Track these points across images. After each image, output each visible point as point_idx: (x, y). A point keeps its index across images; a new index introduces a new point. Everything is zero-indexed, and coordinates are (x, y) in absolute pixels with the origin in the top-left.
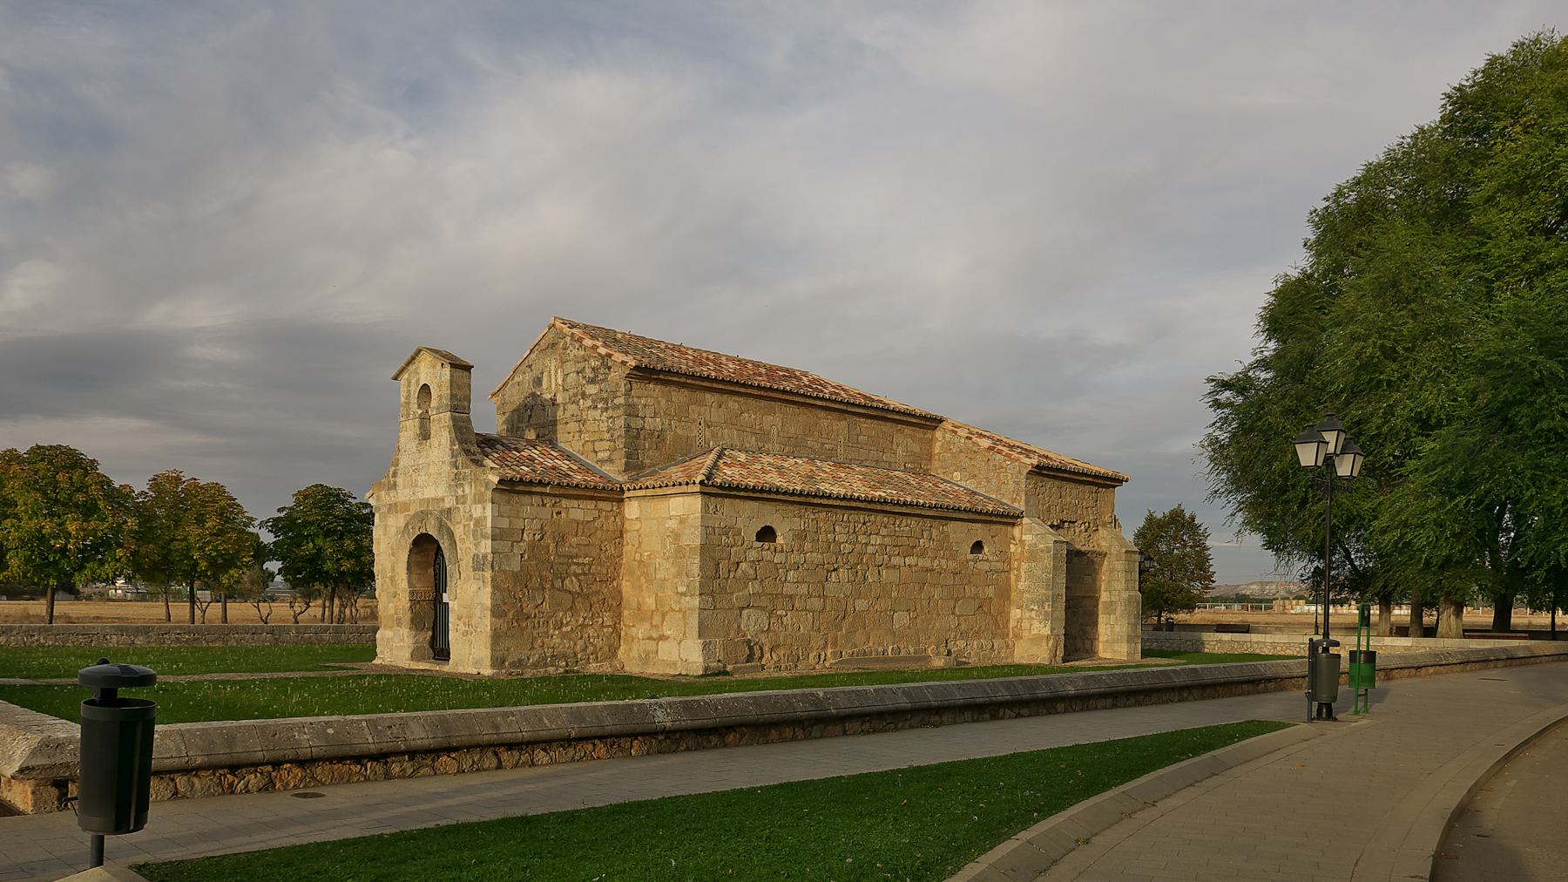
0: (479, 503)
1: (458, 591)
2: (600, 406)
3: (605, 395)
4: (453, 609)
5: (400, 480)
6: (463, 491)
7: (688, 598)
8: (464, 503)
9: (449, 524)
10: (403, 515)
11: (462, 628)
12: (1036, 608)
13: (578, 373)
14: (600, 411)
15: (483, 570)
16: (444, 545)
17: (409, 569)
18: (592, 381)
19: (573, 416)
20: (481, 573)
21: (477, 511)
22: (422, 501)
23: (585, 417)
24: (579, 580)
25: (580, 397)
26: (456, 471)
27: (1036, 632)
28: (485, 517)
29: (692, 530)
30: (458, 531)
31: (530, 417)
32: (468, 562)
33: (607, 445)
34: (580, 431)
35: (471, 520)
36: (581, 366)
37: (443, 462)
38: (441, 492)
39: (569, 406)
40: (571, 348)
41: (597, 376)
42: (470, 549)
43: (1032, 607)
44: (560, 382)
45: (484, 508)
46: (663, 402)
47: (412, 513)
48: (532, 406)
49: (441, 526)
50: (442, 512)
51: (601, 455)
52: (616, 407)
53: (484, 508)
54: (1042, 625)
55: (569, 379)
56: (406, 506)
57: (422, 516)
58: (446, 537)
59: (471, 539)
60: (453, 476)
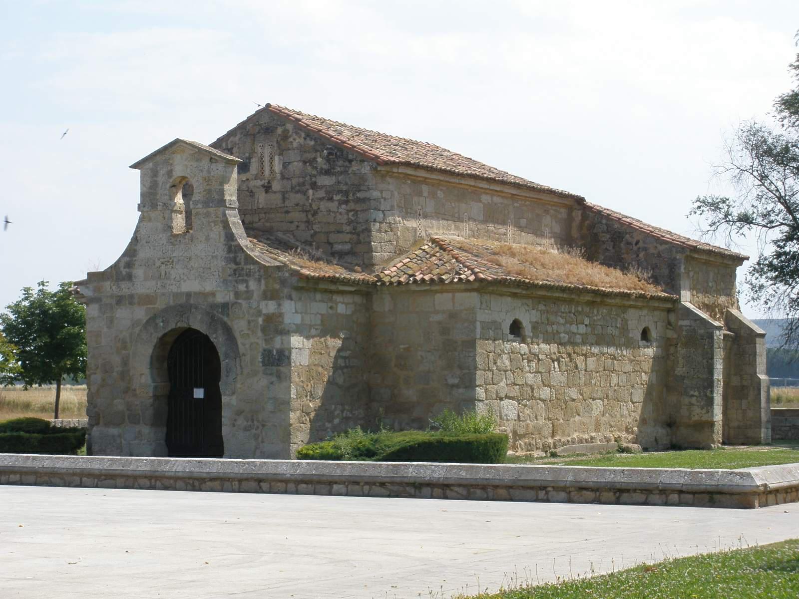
0: (272, 299)
2: (335, 198)
3: (344, 188)
6: (247, 287)
7: (461, 390)
9: (225, 319)
10: (145, 307)
11: (241, 422)
12: (696, 394)
13: (305, 162)
14: (336, 203)
15: (278, 365)
16: (218, 340)
17: (151, 363)
18: (327, 172)
19: (297, 205)
20: (274, 368)
21: (270, 307)
22: (176, 295)
23: (314, 207)
24: (343, 373)
25: (308, 187)
26: (234, 267)
27: (696, 418)
29: (466, 324)
30: (239, 326)
33: (347, 237)
34: (308, 222)
35: (260, 316)
36: (309, 156)
37: (213, 257)
38: (209, 287)
39: (292, 195)
40: (295, 136)
41: (334, 168)
42: (257, 344)
43: (692, 393)
44: (278, 167)
45: (279, 305)
46: (396, 194)
47: (160, 305)
49: (213, 320)
50: (214, 306)
51: (338, 247)
52: (358, 201)
53: (279, 305)
54: (704, 411)
55: (291, 168)
56: (147, 300)
58: (220, 332)
59: (260, 334)
60: (229, 272)
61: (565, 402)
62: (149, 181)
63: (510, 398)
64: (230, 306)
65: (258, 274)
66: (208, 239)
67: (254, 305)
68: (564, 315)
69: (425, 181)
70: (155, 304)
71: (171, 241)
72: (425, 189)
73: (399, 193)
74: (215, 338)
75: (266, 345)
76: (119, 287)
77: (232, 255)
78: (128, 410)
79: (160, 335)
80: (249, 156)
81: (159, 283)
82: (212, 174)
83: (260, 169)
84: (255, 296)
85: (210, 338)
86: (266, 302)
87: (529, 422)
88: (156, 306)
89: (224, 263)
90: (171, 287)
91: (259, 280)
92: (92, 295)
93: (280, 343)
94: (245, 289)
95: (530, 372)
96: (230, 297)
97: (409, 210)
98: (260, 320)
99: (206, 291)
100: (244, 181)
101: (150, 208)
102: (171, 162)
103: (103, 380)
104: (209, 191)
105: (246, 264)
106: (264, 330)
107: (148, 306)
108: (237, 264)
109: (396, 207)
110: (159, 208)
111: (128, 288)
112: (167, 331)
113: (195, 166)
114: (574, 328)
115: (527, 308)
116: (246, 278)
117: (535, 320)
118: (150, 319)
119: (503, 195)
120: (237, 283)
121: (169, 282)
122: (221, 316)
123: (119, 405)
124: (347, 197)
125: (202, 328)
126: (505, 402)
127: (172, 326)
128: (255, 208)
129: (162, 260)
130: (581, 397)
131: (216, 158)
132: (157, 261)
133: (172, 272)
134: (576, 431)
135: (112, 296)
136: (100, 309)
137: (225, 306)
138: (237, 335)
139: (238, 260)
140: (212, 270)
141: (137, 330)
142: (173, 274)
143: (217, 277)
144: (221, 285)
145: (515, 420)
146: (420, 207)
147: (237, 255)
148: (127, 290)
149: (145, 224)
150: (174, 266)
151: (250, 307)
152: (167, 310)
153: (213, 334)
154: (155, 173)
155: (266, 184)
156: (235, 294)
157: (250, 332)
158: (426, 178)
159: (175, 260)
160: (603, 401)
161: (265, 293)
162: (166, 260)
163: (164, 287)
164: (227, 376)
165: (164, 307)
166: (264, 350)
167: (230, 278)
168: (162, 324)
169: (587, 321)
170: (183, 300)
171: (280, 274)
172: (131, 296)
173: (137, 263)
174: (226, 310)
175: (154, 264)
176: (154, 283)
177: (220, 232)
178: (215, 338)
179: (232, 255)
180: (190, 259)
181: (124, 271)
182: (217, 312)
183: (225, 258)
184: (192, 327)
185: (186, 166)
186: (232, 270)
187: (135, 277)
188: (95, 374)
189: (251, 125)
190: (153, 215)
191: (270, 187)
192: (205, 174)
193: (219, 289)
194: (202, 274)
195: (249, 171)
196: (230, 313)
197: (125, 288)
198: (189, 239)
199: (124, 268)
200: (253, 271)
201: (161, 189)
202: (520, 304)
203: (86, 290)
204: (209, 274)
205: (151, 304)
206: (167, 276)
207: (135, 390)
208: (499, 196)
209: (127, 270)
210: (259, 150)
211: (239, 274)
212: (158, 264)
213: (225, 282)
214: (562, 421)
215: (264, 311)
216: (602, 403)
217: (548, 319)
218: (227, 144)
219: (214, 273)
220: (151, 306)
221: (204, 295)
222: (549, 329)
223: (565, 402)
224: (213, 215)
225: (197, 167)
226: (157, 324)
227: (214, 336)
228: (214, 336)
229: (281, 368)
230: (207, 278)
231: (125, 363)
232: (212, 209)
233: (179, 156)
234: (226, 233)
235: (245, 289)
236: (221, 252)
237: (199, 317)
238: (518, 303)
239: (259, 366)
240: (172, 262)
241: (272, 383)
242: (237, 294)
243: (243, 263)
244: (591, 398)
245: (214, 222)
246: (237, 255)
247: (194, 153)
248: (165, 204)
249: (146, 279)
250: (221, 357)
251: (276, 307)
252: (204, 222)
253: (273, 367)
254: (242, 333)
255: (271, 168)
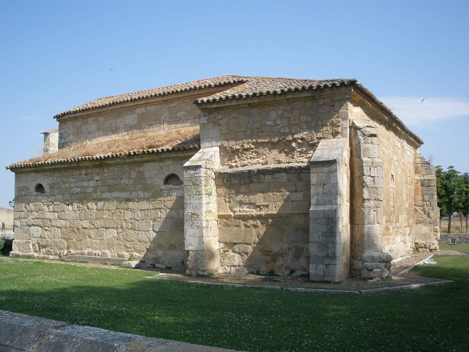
46: (71, 128)
61: (78, 229)
63: (35, 225)
68: (75, 177)
69: (88, 116)
72: (90, 120)
73: (73, 127)
87: (49, 239)
95: (49, 212)
97: (79, 133)
109: (71, 134)
114: (85, 184)
115: (46, 177)
117: (51, 183)
119: (155, 103)
126: (33, 227)
130: (92, 226)
134: (88, 247)
145: (39, 238)
146: (86, 130)
158: (88, 115)
160: (117, 230)
169: (97, 178)
202: (41, 176)
208: (153, 105)
214: (75, 240)
216: (116, 231)
217: (62, 181)
222: (63, 186)
223: (78, 229)
238: (40, 175)
244: (103, 228)
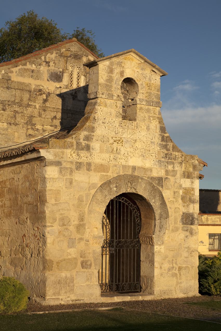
0: (188, 177)
1: (166, 239)
4: (159, 252)
5: (95, 145)
6: (174, 167)
8: (174, 176)
9: (161, 189)
10: (100, 174)
16: (155, 203)
21: (186, 183)
22: (124, 167)
26: (166, 152)
28: (193, 189)
30: (167, 194)
31: (45, 101)
32: (176, 219)
38: (148, 164)
42: (179, 208)
45: (192, 182)
47: (111, 174)
48: (49, 94)
53: (192, 182)
57: (133, 179)
59: (180, 201)
60: (162, 155)
62: (106, 76)
64: (164, 180)
65: (180, 159)
66: (148, 129)
67: (178, 181)
70: (108, 172)
71: (121, 125)
74: (154, 203)
75: (184, 210)
76: (78, 155)
77: (164, 143)
78: (81, 257)
79: (112, 197)
80: (63, 71)
81: (112, 156)
82: (152, 82)
83: (70, 82)
84: (178, 175)
85: (150, 202)
86: (184, 179)
88: (108, 174)
89: (159, 148)
90: (121, 161)
91: (181, 163)
92: (53, 158)
93: (192, 208)
94: (172, 169)
96: (162, 173)
98: (181, 192)
99: (146, 167)
100: (58, 88)
101: (107, 96)
102: (123, 65)
103: (60, 232)
104: (150, 94)
105: (173, 150)
106: (183, 198)
107: (102, 173)
108: (168, 150)
110: (115, 98)
111: (86, 157)
112: (119, 194)
113: (141, 73)
116: (173, 161)
118: (105, 184)
120: (168, 164)
121: (119, 156)
122: (158, 187)
123: (73, 252)
124: (125, 114)
125: (145, 195)
127: (123, 191)
128: (66, 109)
129: (115, 139)
131: (156, 71)
132: (110, 138)
133: (122, 149)
135: (71, 162)
136: (61, 172)
137: (160, 180)
138: (167, 201)
139: (168, 147)
140: (151, 152)
141: (93, 192)
142: (123, 150)
143: (154, 157)
144: (157, 163)
147: (168, 143)
148: (85, 159)
149: (102, 108)
150: (123, 145)
151: (176, 182)
152: (119, 178)
153: (153, 199)
154: (111, 71)
155: (73, 94)
156: (166, 172)
157: (174, 200)
159: (124, 140)
161: (184, 173)
162: (118, 139)
163: (115, 159)
164: (160, 231)
165: (116, 175)
166: (183, 213)
167: (163, 160)
168: (115, 189)
170: (130, 172)
171: (193, 161)
172: (89, 164)
173: (95, 138)
174: (161, 182)
175: (108, 141)
176: (107, 155)
177: (156, 125)
178: (154, 203)
179: (164, 143)
180: (136, 141)
181: (84, 143)
182: (155, 183)
183: (160, 144)
184: (138, 193)
185: (133, 70)
186: (164, 154)
187: (93, 149)
188: (52, 226)
189: (64, 50)
190: (109, 102)
191: (76, 97)
192: (147, 79)
193: (155, 166)
194: (144, 154)
195: (62, 81)
196: (163, 185)
197: (84, 157)
198: (135, 127)
199: (84, 140)
200: (178, 156)
201: (115, 84)
203: (48, 154)
204: (149, 155)
205: (104, 172)
206: (118, 152)
207: (88, 241)
209: (86, 142)
210: (70, 69)
211: (169, 158)
212: (111, 141)
213: (160, 162)
215: (184, 186)
218: (45, 58)
219: (153, 155)
220: (105, 174)
221: (145, 170)
224: (152, 112)
225: (142, 74)
226: (111, 189)
227: (153, 201)
228: (153, 201)
229: (192, 226)
230: (147, 157)
231: (82, 219)
232: (151, 107)
233: (129, 62)
234: (160, 126)
235: (172, 169)
236: (157, 140)
237: (144, 186)
239: (180, 225)
240: (122, 141)
241: (187, 237)
242: (167, 172)
243: (171, 150)
245: (153, 117)
246: (168, 143)
247: (140, 63)
248: (118, 95)
249: (101, 151)
250: (157, 217)
251: (190, 183)
252: (146, 116)
253: (188, 226)
254: (169, 200)
255: (78, 83)
